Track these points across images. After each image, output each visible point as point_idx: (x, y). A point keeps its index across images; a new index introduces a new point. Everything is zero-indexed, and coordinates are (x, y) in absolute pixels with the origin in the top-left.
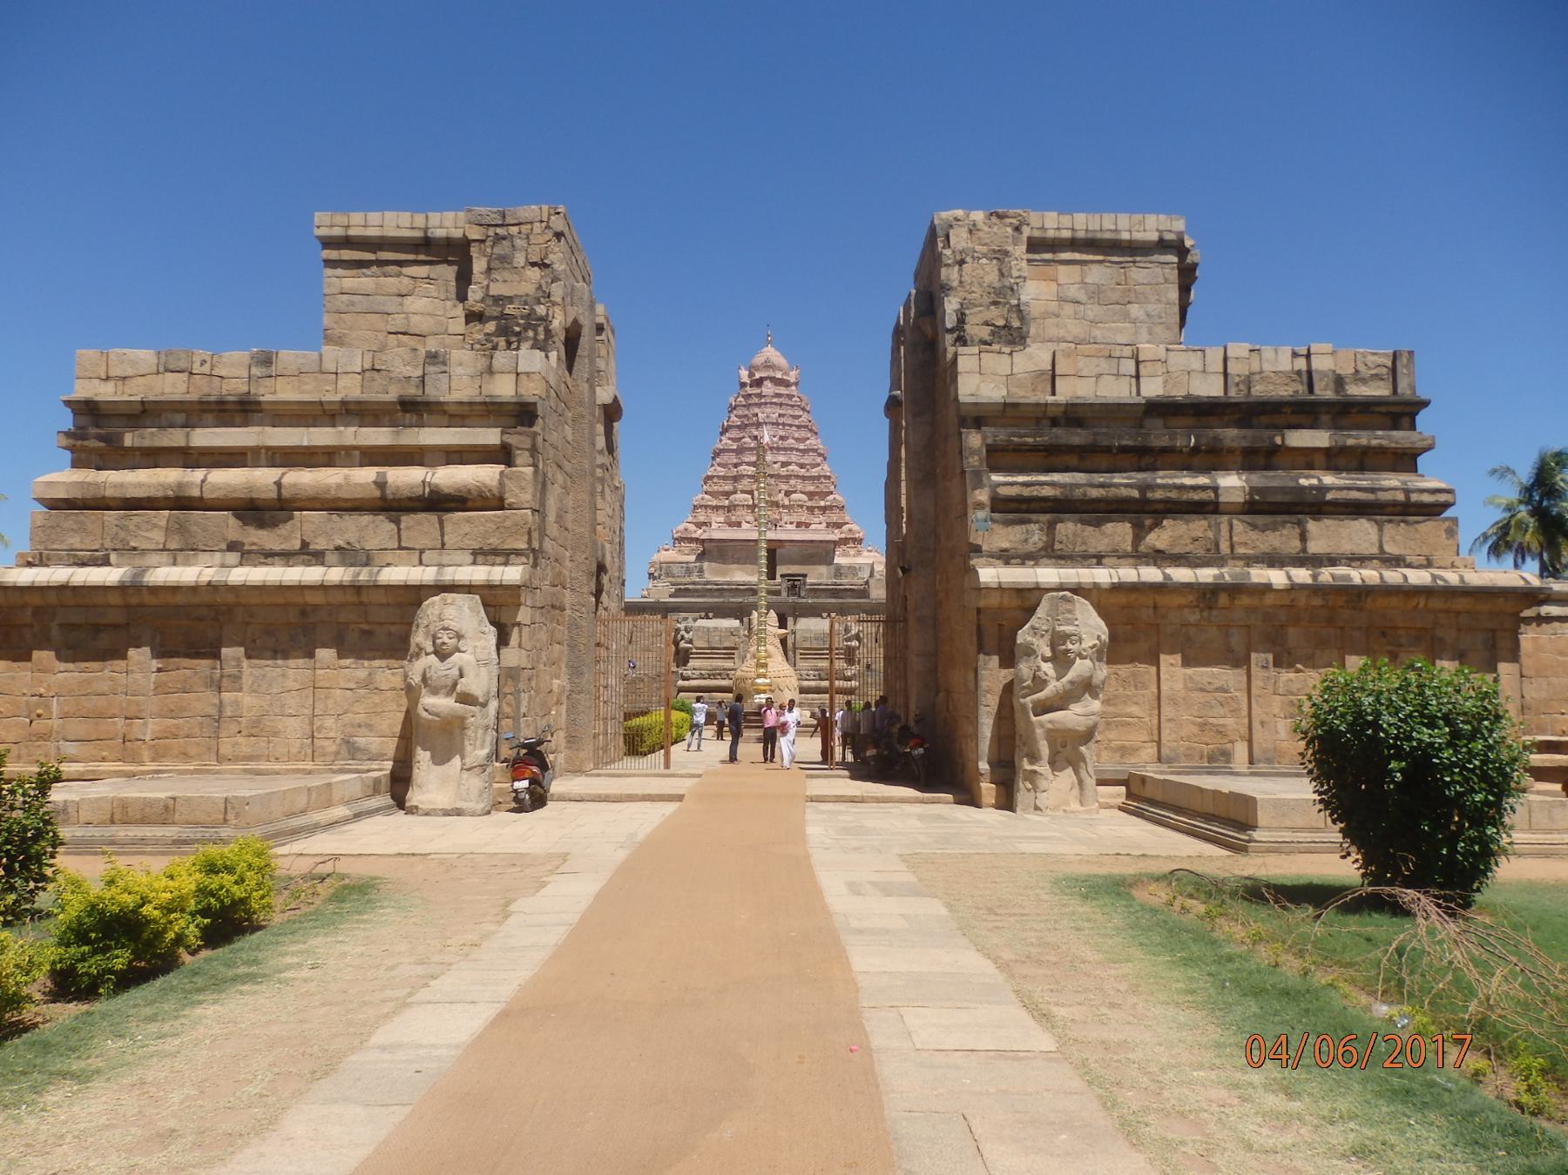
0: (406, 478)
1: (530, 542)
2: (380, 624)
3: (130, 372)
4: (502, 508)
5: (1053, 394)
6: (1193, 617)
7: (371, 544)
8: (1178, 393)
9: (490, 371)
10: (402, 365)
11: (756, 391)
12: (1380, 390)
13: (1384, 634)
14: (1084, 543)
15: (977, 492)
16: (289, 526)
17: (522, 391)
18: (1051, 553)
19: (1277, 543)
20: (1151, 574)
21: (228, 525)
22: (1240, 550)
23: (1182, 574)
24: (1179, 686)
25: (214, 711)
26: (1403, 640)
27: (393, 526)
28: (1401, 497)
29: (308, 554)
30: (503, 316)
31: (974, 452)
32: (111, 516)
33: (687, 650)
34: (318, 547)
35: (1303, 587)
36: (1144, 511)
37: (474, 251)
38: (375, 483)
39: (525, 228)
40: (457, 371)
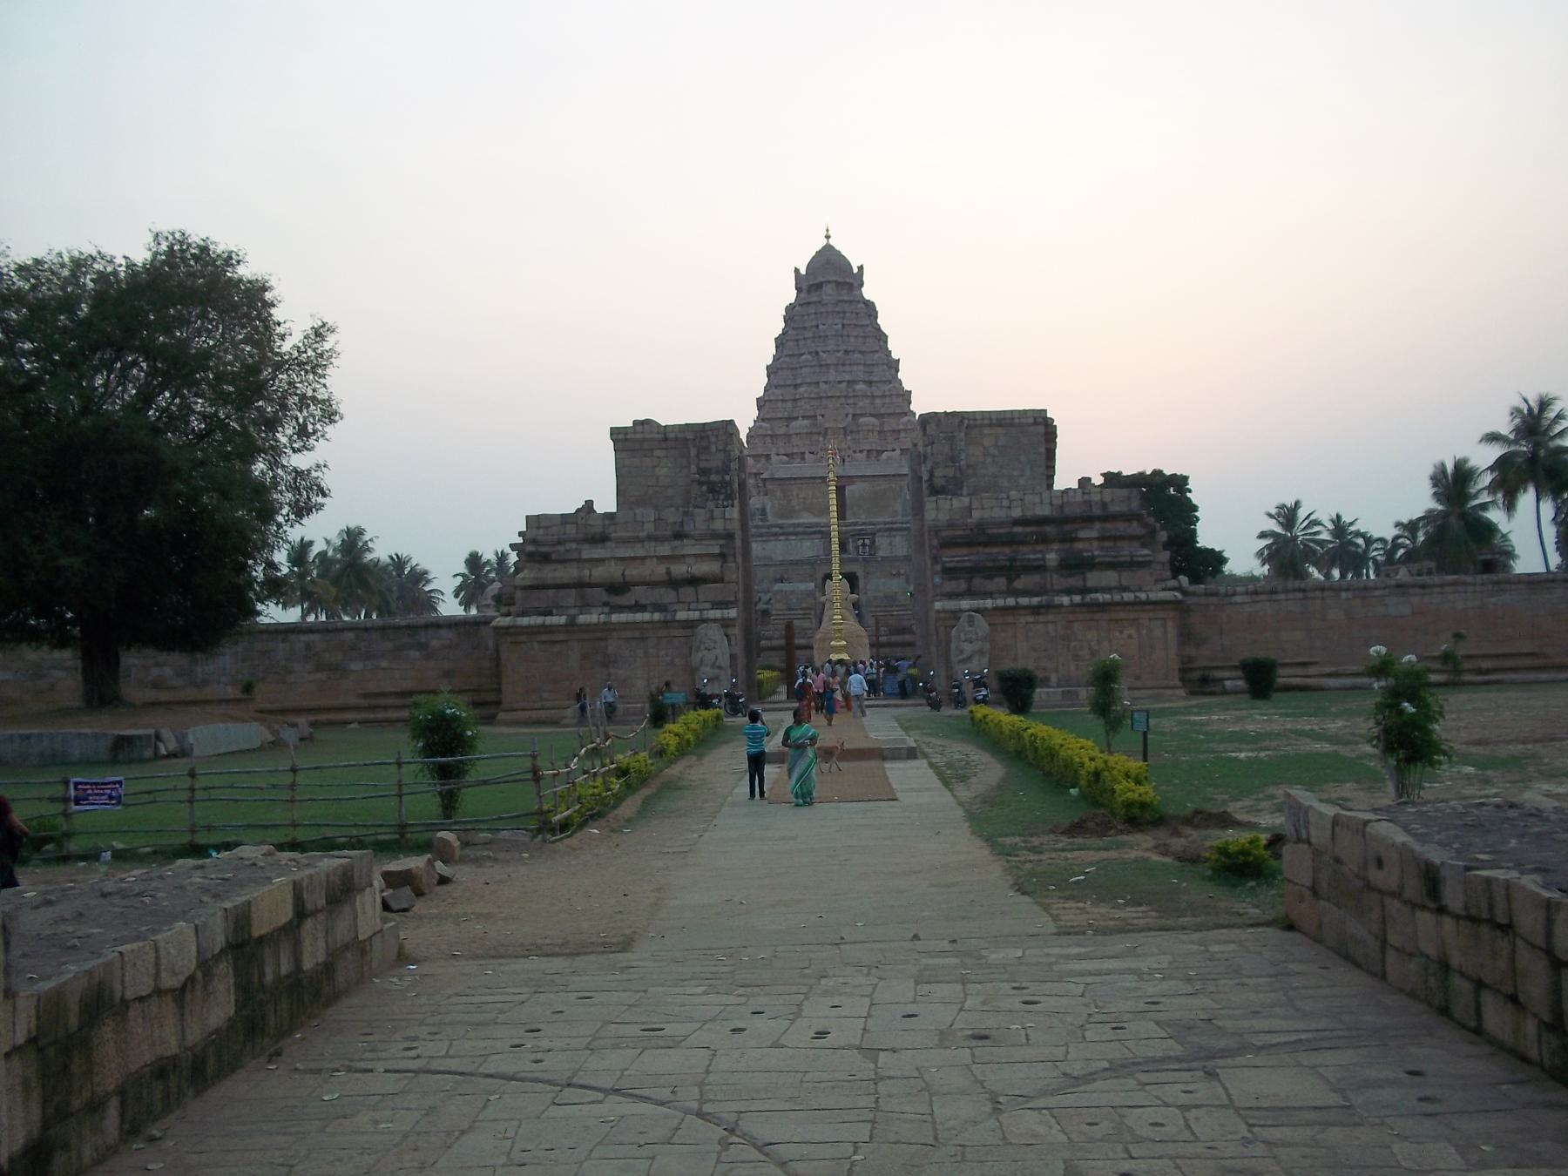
0: (679, 570)
4: (722, 581)
6: (1031, 619)
7: (666, 600)
8: (1029, 514)
9: (712, 518)
10: (672, 516)
18: (970, 593)
20: (1011, 601)
23: (1024, 601)
29: (638, 607)
30: (708, 483)
32: (551, 592)
33: (766, 613)
35: (1077, 605)
36: (1011, 570)
40: (698, 519)
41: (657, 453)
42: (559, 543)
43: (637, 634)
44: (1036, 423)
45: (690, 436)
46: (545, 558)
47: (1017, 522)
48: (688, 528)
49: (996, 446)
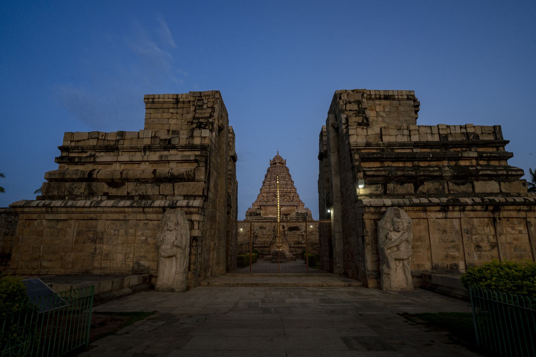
0: (163, 170)
1: (203, 192)
2: (151, 220)
3: (80, 139)
4: (195, 181)
5: (382, 141)
6: (440, 215)
7: (150, 193)
11: (275, 165)
12: (491, 138)
13: (508, 220)
14: (397, 191)
15: (359, 174)
16: (124, 187)
17: (203, 142)
18: (385, 194)
19: (464, 189)
21: (105, 188)
22: (452, 192)
24: (437, 241)
25: (93, 251)
26: (515, 223)
27: (158, 188)
28: (505, 173)
31: (356, 160)
32: (67, 184)
34: (133, 195)
37: (191, 103)
38: (153, 173)
39: (207, 98)
40: (181, 136)
41: (171, 110)
42: (83, 151)
43: (121, 216)
44: (408, 99)
45: (191, 99)
46: (71, 161)
47: (416, 145)
48: (175, 142)
49: (384, 111)
